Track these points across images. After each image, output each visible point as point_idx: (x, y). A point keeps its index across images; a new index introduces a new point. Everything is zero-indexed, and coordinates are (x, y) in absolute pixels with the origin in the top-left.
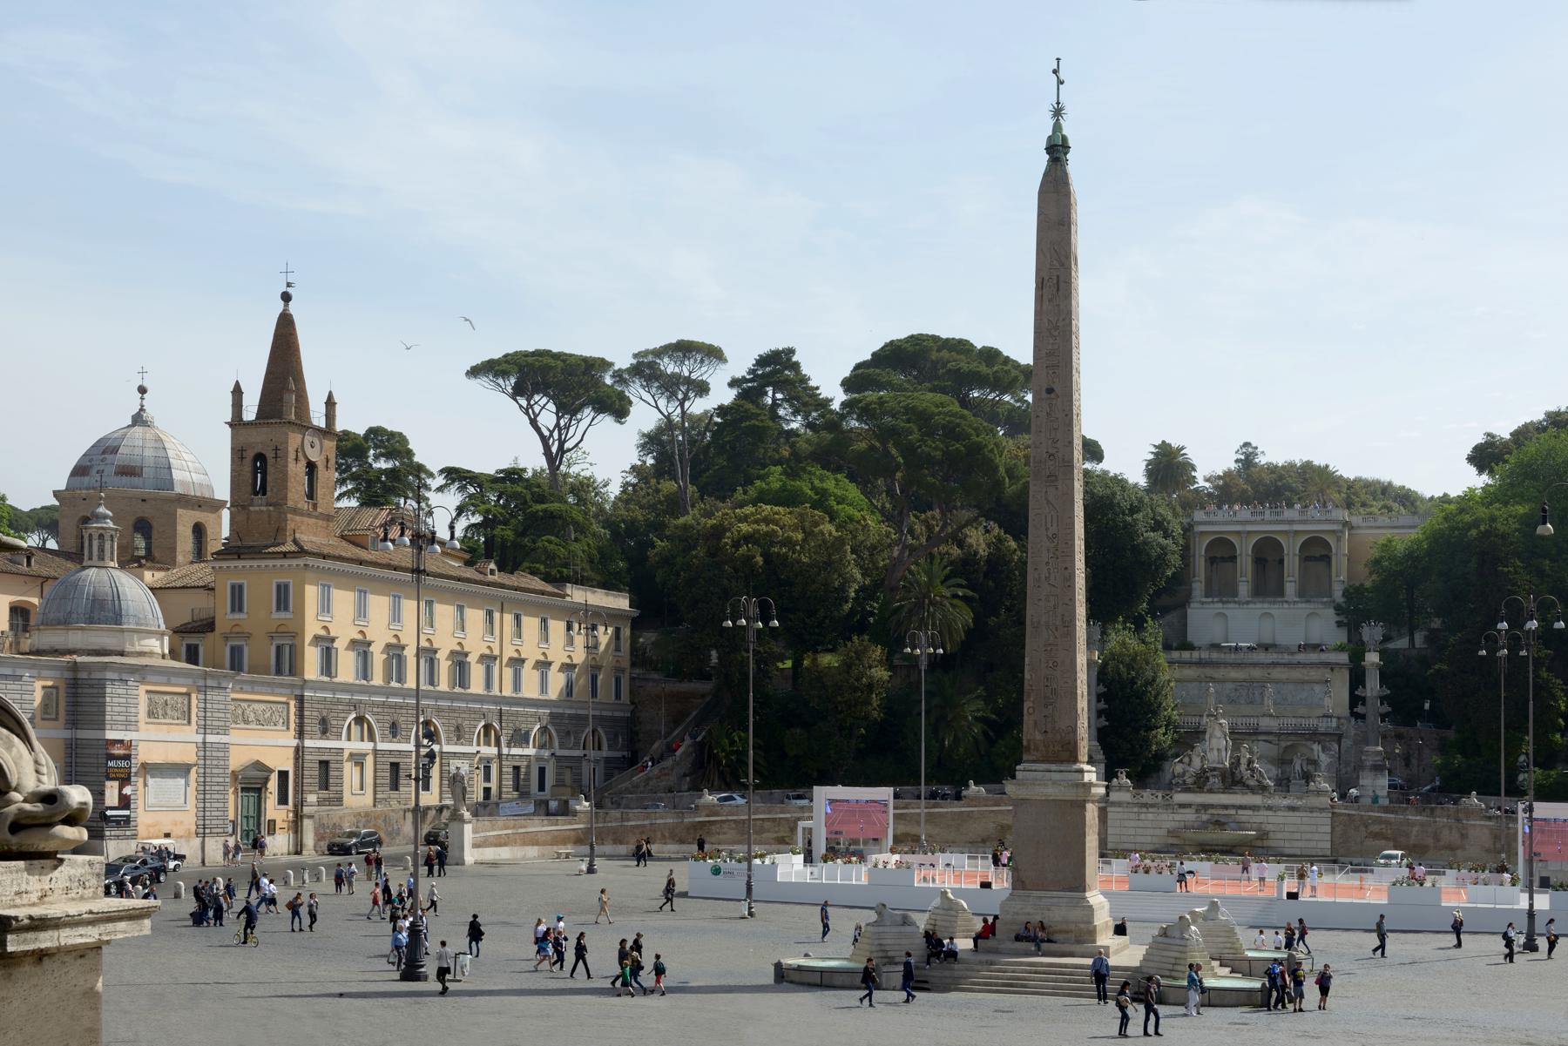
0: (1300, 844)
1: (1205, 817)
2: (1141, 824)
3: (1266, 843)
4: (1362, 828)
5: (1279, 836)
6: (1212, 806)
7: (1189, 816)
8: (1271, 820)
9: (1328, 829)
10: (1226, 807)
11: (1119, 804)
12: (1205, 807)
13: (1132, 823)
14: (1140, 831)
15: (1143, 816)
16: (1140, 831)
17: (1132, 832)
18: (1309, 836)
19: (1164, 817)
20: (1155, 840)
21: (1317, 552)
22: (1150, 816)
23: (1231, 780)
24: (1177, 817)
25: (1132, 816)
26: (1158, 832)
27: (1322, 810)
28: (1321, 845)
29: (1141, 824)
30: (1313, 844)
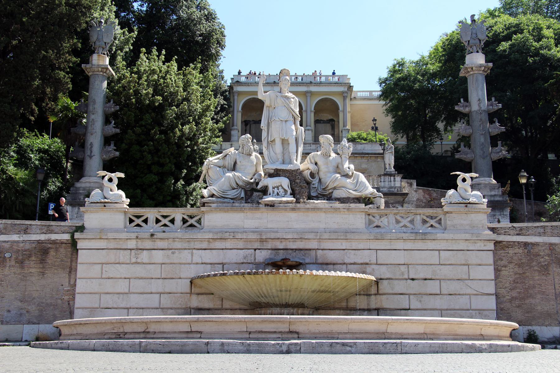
2: (139, 271)
5: (400, 287)
9: (490, 273)
11: (101, 234)
13: (122, 271)
14: (138, 285)
15: (144, 256)
17: (122, 286)
18: (454, 287)
19: (185, 256)
21: (326, 116)
22: (158, 256)
23: (304, 188)
25: (123, 256)
26: (171, 286)
29: (139, 271)
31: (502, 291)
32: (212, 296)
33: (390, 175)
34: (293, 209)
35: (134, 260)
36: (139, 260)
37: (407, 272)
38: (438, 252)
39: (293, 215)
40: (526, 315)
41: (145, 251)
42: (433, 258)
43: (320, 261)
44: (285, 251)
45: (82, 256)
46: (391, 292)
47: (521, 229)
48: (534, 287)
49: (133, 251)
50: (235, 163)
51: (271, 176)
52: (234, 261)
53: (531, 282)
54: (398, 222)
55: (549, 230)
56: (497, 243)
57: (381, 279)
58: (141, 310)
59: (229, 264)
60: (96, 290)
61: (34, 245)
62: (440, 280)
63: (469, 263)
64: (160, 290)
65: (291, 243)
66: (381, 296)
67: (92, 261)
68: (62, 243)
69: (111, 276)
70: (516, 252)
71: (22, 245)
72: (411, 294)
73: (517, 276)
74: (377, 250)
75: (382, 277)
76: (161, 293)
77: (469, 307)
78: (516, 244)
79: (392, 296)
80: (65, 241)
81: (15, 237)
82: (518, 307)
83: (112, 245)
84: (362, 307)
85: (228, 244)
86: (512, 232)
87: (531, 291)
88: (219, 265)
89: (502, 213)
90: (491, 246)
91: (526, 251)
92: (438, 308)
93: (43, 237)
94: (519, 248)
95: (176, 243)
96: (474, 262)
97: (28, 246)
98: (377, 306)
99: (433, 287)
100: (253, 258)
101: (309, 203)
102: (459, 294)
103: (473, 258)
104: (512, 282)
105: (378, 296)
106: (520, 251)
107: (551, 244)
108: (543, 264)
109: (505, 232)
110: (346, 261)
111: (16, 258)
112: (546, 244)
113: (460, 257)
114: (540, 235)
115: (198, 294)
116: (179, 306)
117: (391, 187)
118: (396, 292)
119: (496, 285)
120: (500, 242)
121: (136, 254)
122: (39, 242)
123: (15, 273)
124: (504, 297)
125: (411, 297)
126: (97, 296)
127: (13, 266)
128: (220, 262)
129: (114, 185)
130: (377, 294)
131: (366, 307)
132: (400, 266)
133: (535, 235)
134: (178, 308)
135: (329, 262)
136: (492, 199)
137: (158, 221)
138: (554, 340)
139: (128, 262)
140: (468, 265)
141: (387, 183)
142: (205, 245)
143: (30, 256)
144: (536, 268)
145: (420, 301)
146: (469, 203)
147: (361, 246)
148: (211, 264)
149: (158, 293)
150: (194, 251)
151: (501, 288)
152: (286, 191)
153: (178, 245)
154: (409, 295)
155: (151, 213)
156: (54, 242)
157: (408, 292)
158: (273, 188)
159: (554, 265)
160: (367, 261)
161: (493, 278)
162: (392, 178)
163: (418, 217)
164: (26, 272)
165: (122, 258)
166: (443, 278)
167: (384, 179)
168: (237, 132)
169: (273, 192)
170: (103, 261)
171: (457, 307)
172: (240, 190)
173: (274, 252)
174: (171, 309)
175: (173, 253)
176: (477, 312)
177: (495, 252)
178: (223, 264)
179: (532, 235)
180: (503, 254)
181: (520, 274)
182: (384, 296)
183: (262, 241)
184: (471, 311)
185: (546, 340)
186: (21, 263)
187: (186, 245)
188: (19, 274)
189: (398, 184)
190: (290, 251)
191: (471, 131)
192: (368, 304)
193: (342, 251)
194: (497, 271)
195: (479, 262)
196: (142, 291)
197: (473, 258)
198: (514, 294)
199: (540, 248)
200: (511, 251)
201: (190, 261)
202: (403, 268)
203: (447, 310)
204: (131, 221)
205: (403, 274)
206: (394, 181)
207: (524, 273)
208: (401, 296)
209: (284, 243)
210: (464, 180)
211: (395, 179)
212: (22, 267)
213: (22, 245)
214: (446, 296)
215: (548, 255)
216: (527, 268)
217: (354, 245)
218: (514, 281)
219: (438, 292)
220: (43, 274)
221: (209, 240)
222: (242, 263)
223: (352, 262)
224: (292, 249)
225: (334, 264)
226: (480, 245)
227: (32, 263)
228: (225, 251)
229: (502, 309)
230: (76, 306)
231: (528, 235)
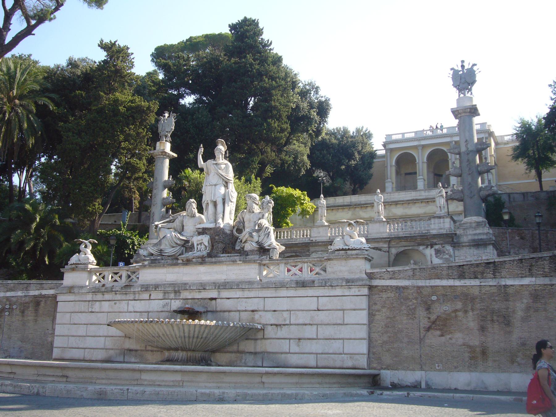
0: (315, 347)
1: (176, 304)
2: (93, 318)
3: (261, 346)
4: (421, 313)
6: (185, 286)
7: (156, 304)
8: (270, 304)
9: (363, 317)
10: (203, 287)
11: (71, 290)
12: (177, 289)
15: (97, 307)
16: (92, 330)
17: (82, 330)
20: (109, 343)
22: (106, 306)
24: (139, 306)
25: (83, 307)
27: (349, 283)
28: (350, 347)
29: (93, 318)
30: (336, 346)
31: (375, 336)
35: (90, 310)
36: (93, 310)
37: (289, 318)
38: (316, 298)
39: (202, 269)
40: (395, 359)
41: (97, 303)
43: (218, 309)
44: (193, 300)
45: (61, 307)
46: (274, 336)
47: (394, 272)
51: (200, 234)
52: (156, 309)
53: (400, 326)
54: (289, 270)
56: (371, 288)
57: (267, 324)
58: (92, 350)
59: (152, 312)
60: (66, 334)
61: (31, 299)
62: (317, 325)
63: (344, 308)
64: (106, 334)
66: (266, 341)
67: (65, 311)
68: (49, 297)
69: (76, 323)
70: (389, 296)
71: (24, 299)
72: (292, 339)
73: (389, 320)
74: (265, 298)
75: (268, 323)
76: (106, 336)
77: (341, 351)
78: (389, 288)
79: (275, 340)
80: (51, 296)
81: (20, 293)
82: (388, 351)
83: (77, 298)
84: (250, 351)
86: (386, 276)
88: (145, 314)
89: (485, 251)
90: (365, 291)
92: (314, 352)
93: (37, 293)
94: (391, 292)
95: (117, 295)
96: (349, 307)
97: (27, 299)
98: (262, 350)
100: (169, 307)
101: (220, 257)
102: (334, 339)
103: (348, 303)
104: (384, 327)
105: (263, 340)
106: (392, 295)
107: (419, 287)
108: (411, 307)
109: (381, 276)
110: (239, 309)
111: (20, 309)
112: (414, 287)
113: (336, 303)
116: (117, 348)
118: (278, 337)
120: (376, 286)
122: (35, 296)
123: (18, 320)
124: (377, 341)
126: (66, 338)
127: (18, 315)
128: (146, 310)
129: (89, 250)
130: (264, 338)
131: (253, 351)
133: (406, 279)
134: (116, 349)
135: (226, 309)
136: (476, 237)
138: (416, 384)
139: (87, 311)
140: (343, 310)
141: (437, 225)
143: (28, 307)
144: (405, 312)
145: (298, 346)
146: (349, 249)
148: (140, 312)
150: (130, 302)
151: (374, 333)
154: (290, 339)
156: (44, 296)
157: (288, 337)
158: (198, 245)
159: (421, 308)
161: (365, 321)
162: (442, 220)
163: (306, 264)
164: (25, 319)
165: (83, 308)
166: (320, 323)
168: (391, 184)
170: (72, 311)
171: (331, 351)
172: (178, 247)
174: (112, 349)
175: (115, 304)
176: (348, 356)
177: (369, 296)
178: (148, 312)
180: (377, 299)
182: (269, 341)
184: (343, 355)
185: (409, 384)
186: (23, 312)
188: (21, 321)
190: (196, 301)
191: (460, 172)
193: (236, 300)
194: (371, 315)
195: (353, 307)
196: (93, 334)
197: (348, 303)
198: (385, 338)
200: (384, 295)
201: (126, 310)
202: (286, 314)
203: (322, 354)
205: (285, 320)
206: (444, 223)
208: (283, 341)
209: (192, 294)
212: (23, 316)
213: (24, 299)
214: (321, 341)
215: (416, 298)
216: (398, 312)
218: (386, 325)
219: (315, 337)
220: (36, 321)
222: (162, 311)
223: (244, 309)
224: (198, 299)
225: (229, 311)
226: (355, 291)
227: (29, 313)
229: (374, 353)
230: (55, 346)
231: (400, 279)
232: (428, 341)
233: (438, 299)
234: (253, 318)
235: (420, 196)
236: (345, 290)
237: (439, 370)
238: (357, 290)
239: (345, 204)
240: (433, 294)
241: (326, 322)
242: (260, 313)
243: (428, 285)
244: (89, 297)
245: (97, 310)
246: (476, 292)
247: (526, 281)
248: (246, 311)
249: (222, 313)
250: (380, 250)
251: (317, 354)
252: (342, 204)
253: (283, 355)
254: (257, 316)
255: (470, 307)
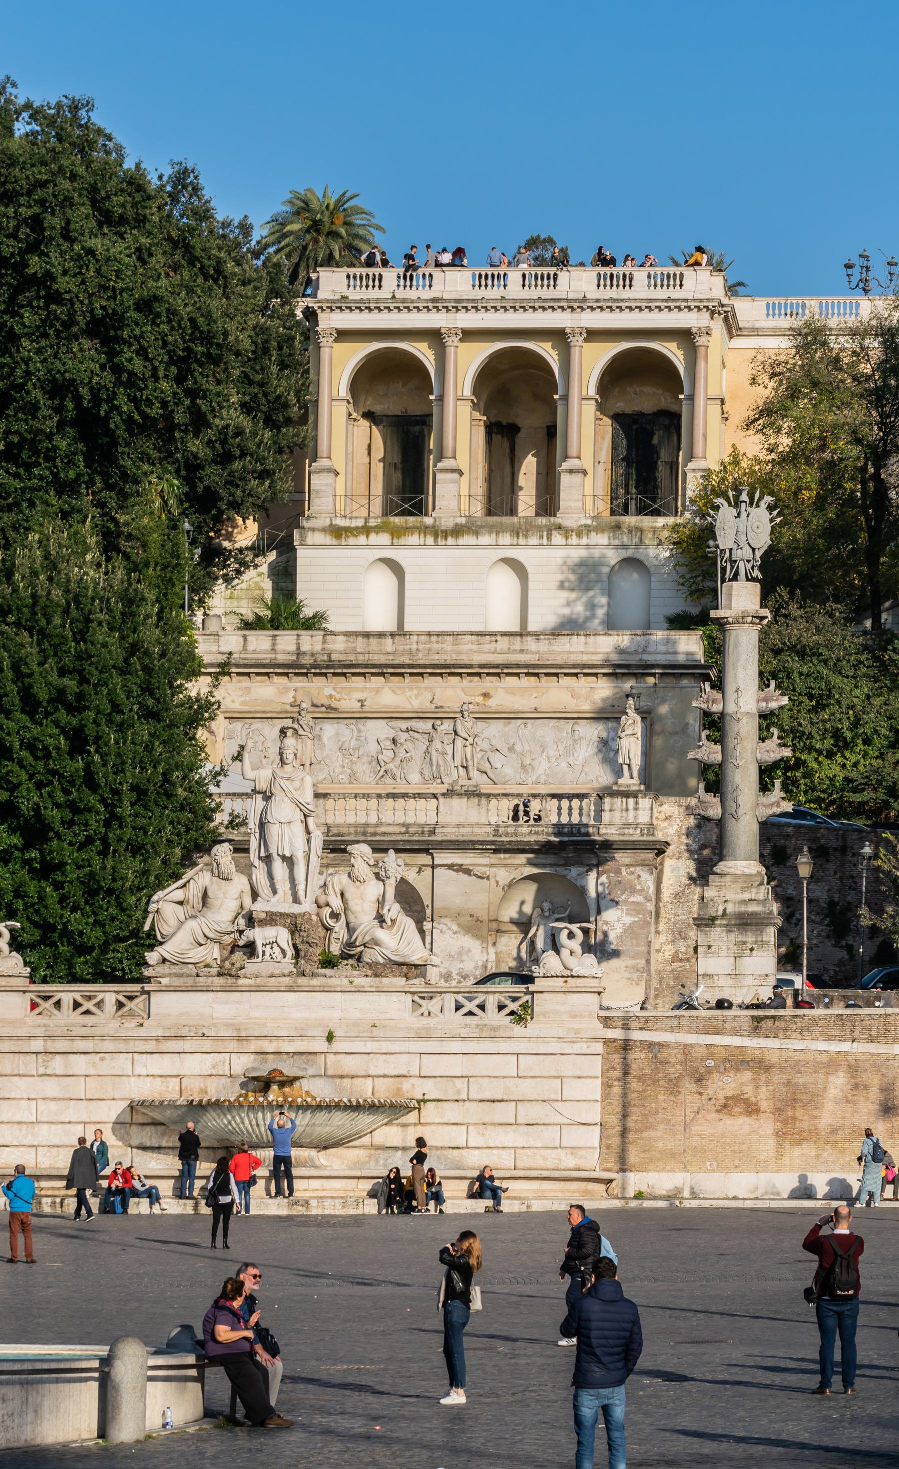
1: (242, 1064)
8: (432, 1065)
9: (595, 1089)
15: (57, 1064)
19: (122, 1063)
32: (163, 1127)
33: (627, 795)
34: (290, 989)
35: (41, 1071)
36: (49, 1071)
41: (58, 1056)
42: (509, 1066)
48: (657, 1112)
49: (40, 1056)
50: (205, 895)
55: (684, 1022)
59: (189, 1076)
62: (516, 1101)
65: (286, 1043)
78: (638, 1043)
85: (187, 1045)
87: (651, 1119)
89: (760, 939)
90: (599, 1047)
91: (651, 1055)
92: (510, 1145)
95: (106, 1043)
99: (505, 1113)
100: (227, 1068)
103: (568, 1066)
106: (643, 1056)
107: (686, 1046)
108: (673, 1076)
110: (371, 1072)
114: (672, 1030)
115: (143, 1124)
117: (627, 825)
119: (603, 1108)
121: (44, 1061)
125: (470, 1128)
131: (400, 1145)
132: (455, 1080)
135: (344, 1073)
136: (743, 909)
137: (77, 1005)
141: (617, 814)
142: (151, 1046)
147: (395, 1047)
148: (161, 1076)
149: (80, 1123)
150: (136, 1056)
152: (284, 952)
153: (109, 1046)
154: (468, 1125)
155: (68, 993)
159: (687, 1078)
160: (405, 1073)
161: (599, 1098)
162: (631, 801)
167: (612, 804)
169: (264, 952)
173: (260, 1057)
175: (102, 1059)
178: (181, 1077)
179: (662, 1029)
181: (639, 1092)
182: (428, 1128)
183: (240, 1039)
187: (121, 1047)
189: (643, 817)
190: (285, 1057)
192: (404, 1140)
195: (578, 1074)
197: (568, 1066)
199: (670, 1051)
202: (461, 1084)
204: (34, 1006)
205: (458, 1092)
206: (636, 809)
207: (644, 1091)
208: (455, 1127)
209: (275, 1044)
210: (571, 935)
211: (637, 803)
215: (681, 1063)
217: (385, 1046)
221: (157, 1039)
225: (353, 1077)
228: (182, 1055)
231: (656, 1030)
232: (695, 1129)
233: (716, 1067)
234: (399, 1091)
235: (522, 651)
236: (565, 1045)
237: (713, 1171)
238: (584, 1045)
239: (281, 658)
240: (710, 1056)
241: (532, 1097)
242: (413, 1080)
243: (701, 1042)
244: (37, 1045)
245: (59, 1071)
246: (774, 1058)
247: (845, 1047)
248: (385, 1076)
249: (338, 1081)
250: (468, 872)
251: (515, 1148)
252: (267, 658)
253: (456, 1152)
254: (406, 1085)
255: (763, 1079)
